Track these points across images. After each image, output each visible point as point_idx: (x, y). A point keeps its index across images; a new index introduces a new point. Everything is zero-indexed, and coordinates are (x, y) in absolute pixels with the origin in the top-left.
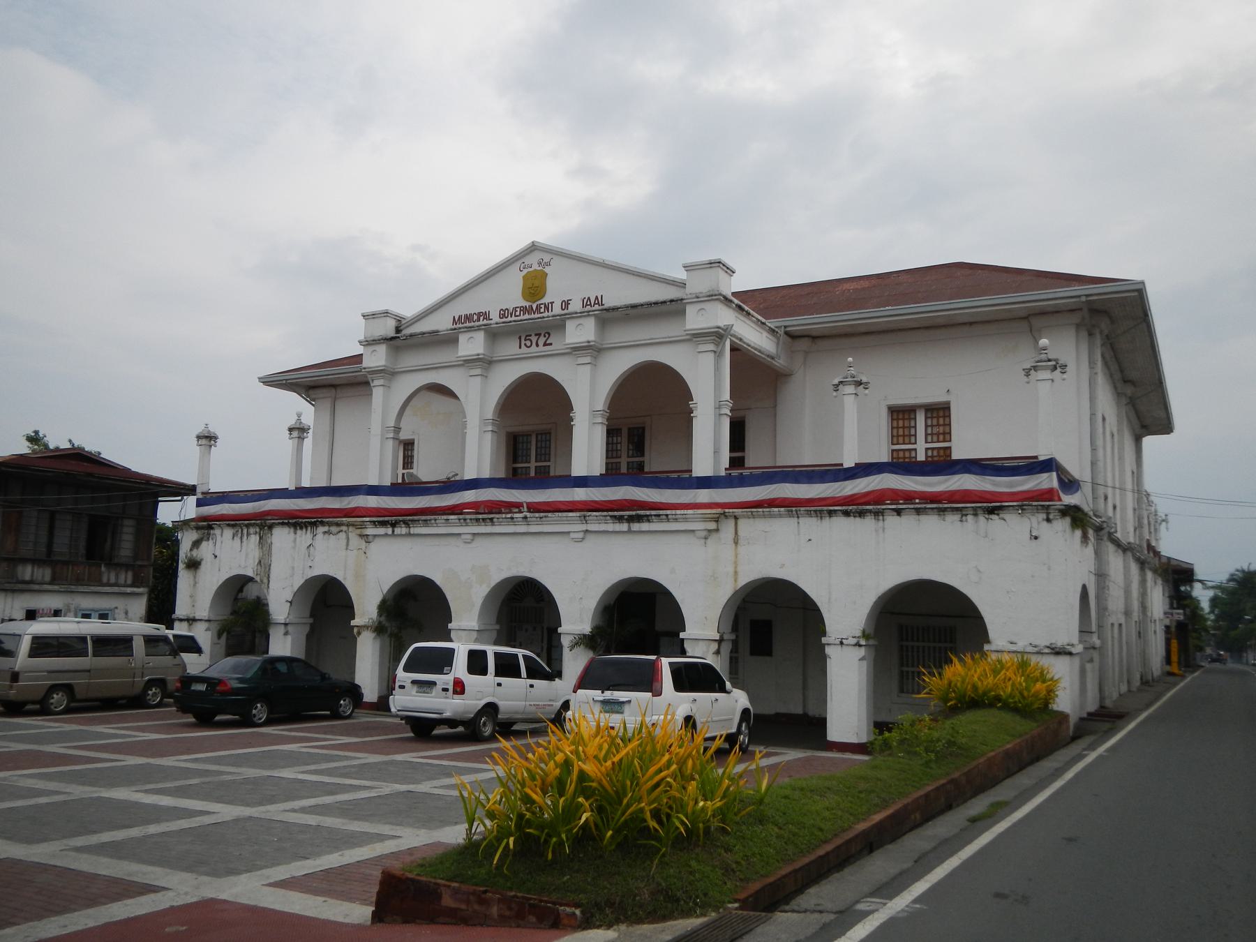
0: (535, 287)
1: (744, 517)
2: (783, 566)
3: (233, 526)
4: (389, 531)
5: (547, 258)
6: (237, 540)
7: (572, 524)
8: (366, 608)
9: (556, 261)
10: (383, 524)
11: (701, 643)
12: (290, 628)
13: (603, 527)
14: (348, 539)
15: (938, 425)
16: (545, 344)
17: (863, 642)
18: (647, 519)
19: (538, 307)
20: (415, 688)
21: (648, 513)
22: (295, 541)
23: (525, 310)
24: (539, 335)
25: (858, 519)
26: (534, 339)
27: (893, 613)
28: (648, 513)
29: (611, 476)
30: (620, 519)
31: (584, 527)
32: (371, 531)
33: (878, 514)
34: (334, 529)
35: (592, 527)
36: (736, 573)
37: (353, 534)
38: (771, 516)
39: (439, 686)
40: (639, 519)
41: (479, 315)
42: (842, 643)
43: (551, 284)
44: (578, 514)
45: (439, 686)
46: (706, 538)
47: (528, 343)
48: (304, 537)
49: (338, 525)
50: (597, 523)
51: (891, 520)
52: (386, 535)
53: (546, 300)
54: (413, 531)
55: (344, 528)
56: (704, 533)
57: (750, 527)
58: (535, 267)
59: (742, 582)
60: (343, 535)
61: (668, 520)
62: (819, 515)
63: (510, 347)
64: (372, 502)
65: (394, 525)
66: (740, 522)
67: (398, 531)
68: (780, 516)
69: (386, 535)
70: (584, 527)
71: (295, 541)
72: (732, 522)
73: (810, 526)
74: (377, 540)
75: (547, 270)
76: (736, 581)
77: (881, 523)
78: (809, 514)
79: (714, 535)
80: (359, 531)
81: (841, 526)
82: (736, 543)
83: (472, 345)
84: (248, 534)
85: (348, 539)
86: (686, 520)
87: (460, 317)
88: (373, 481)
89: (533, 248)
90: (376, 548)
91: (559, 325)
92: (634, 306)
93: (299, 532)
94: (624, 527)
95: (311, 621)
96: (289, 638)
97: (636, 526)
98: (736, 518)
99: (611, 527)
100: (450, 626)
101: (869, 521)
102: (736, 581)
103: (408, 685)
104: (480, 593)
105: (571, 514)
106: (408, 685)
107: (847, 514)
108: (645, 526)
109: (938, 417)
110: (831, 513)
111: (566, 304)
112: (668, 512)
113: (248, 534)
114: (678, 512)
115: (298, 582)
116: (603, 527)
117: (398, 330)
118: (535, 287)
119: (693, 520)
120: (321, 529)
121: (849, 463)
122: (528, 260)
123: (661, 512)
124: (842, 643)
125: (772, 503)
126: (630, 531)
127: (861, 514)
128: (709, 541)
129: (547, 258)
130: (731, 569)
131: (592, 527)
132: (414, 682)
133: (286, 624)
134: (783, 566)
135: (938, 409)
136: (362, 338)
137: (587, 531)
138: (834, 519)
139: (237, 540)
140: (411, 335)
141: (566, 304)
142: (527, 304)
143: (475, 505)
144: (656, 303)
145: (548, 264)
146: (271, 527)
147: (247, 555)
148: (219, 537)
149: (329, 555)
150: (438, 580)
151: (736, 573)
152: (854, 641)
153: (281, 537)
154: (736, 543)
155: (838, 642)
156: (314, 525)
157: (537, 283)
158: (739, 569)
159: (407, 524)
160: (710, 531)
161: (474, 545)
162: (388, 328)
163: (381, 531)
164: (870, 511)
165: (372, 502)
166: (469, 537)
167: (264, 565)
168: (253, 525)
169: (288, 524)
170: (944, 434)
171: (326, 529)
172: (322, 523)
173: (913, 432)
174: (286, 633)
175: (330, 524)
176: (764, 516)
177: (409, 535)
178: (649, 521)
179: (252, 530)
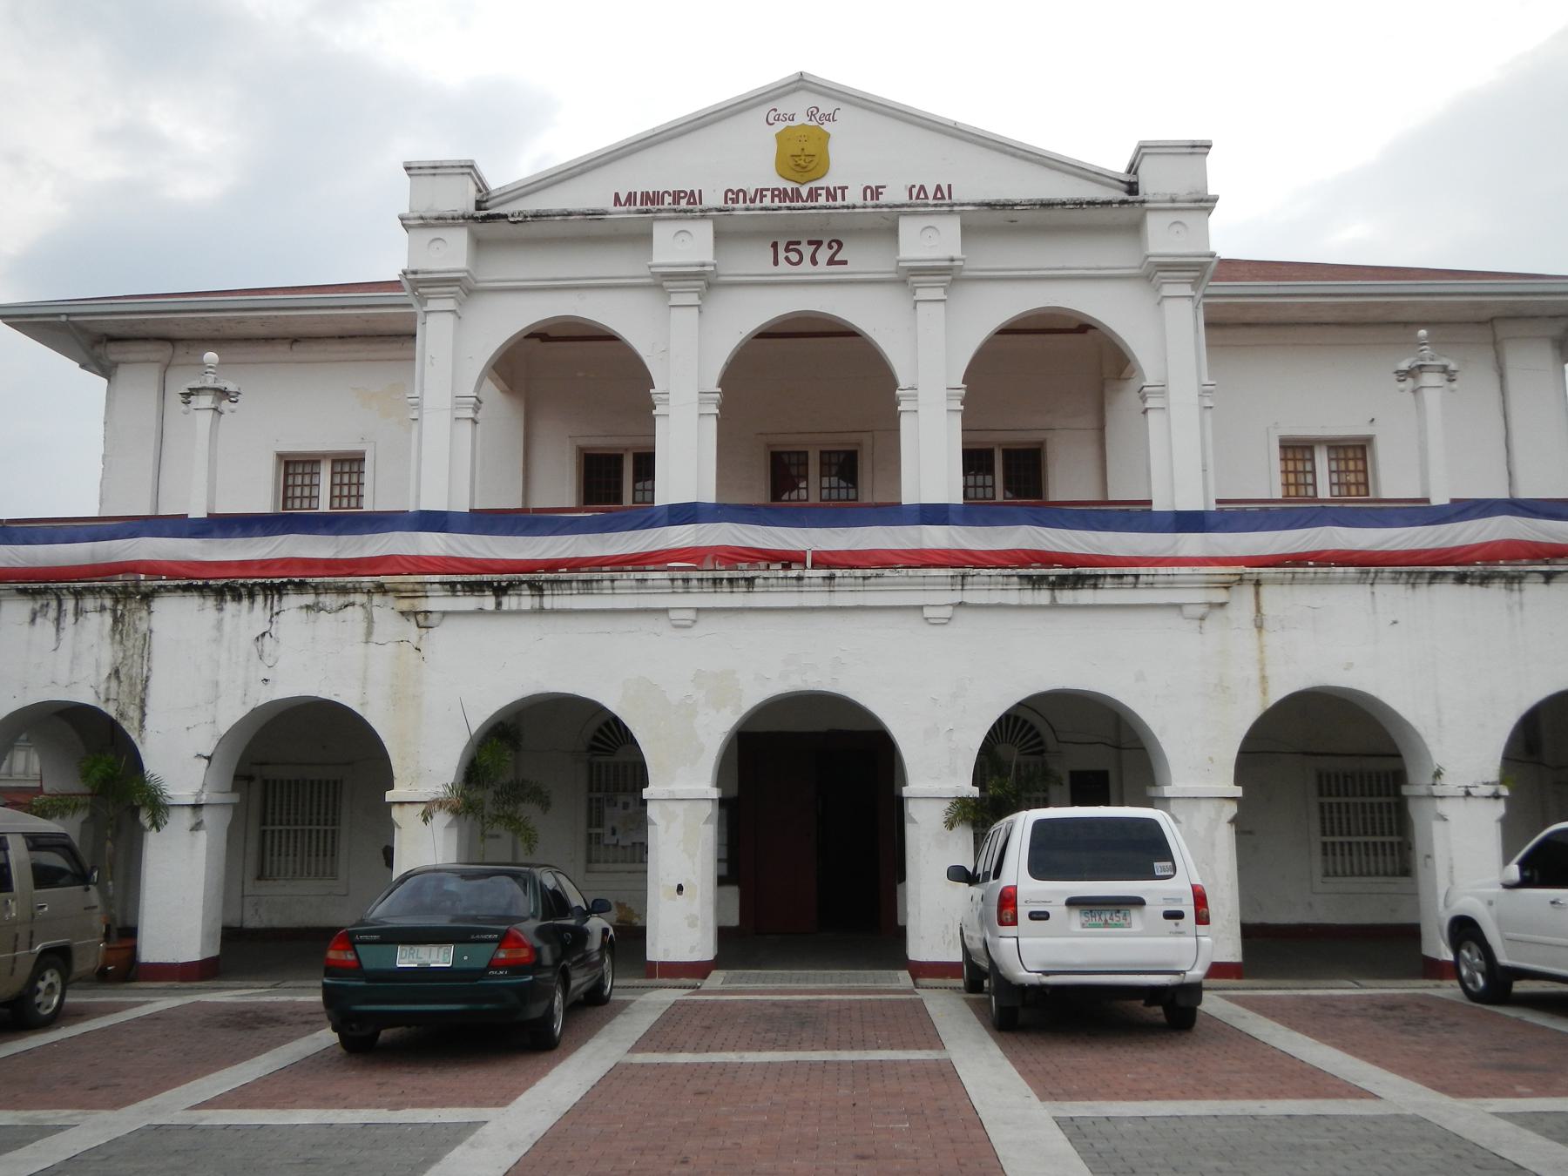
0: (803, 157)
1: (1274, 582)
2: (1349, 666)
3: (35, 594)
4: (489, 602)
5: (826, 107)
7: (936, 590)
8: (426, 760)
9: (847, 114)
10: (474, 588)
11: (1204, 805)
12: (206, 815)
13: (997, 597)
14: (370, 621)
15: (1347, 471)
16: (831, 262)
17: (1504, 791)
18: (1094, 582)
19: (813, 194)
20: (1076, 918)
21: (1100, 571)
23: (782, 194)
24: (819, 244)
25: (1477, 588)
26: (807, 250)
27: (1305, 753)
28: (1100, 571)
29: (972, 512)
30: (1036, 582)
31: (957, 597)
32: (437, 602)
33: (1512, 580)
34: (329, 600)
35: (970, 597)
36: (1264, 678)
37: (385, 611)
38: (1327, 581)
39: (1154, 908)
40: (1077, 582)
41: (677, 196)
42: (1468, 794)
43: (836, 151)
44: (951, 572)
45: (1154, 908)
46: (1202, 619)
47: (794, 257)
48: (246, 618)
49: (343, 590)
50: (984, 589)
51: (1534, 591)
52: (480, 611)
53: (829, 181)
54: (548, 602)
55: (359, 598)
56: (1201, 610)
57: (1281, 599)
58: (801, 119)
59: (1277, 693)
60: (355, 614)
61: (1135, 586)
62: (1413, 580)
63: (756, 261)
64: (433, 544)
65: (500, 591)
66: (1266, 591)
67: (509, 602)
68: (1343, 581)
69: (480, 611)
70: (957, 597)
71: (220, 622)
72: (1248, 591)
73: (1392, 597)
74: (449, 622)
75: (827, 127)
76: (1264, 692)
77: (1516, 595)
78: (1395, 580)
79: (1218, 613)
80: (405, 605)
81: (1447, 598)
82: (1260, 627)
83: (682, 245)
84: (78, 612)
85: (370, 621)
86: (1170, 585)
87: (631, 198)
88: (434, 501)
89: (801, 84)
90: (443, 639)
91: (882, 225)
92: (1047, 205)
93: (230, 606)
94: (1043, 597)
95: (235, 798)
96: (202, 835)
97: (1066, 596)
98: (1258, 583)
99: (1013, 597)
100: (646, 793)
101: (1496, 591)
102: (1264, 692)
103: (1058, 910)
104: (715, 729)
105: (934, 572)
106: (1058, 910)
107: (1461, 579)
108: (1085, 596)
109: (1347, 460)
110: (1435, 578)
112: (1142, 570)
113: (78, 612)
114: (1162, 570)
115: (232, 712)
116: (997, 597)
117: (479, 205)
118: (803, 157)
119: (1188, 585)
120: (292, 601)
121: (1440, 498)
122: (784, 106)
123: (1127, 570)
124: (1468, 794)
125: (1299, 560)
126: (1053, 605)
127: (1485, 580)
128: (1207, 623)
129: (826, 107)
130: (1254, 674)
131: (970, 597)
132: (1072, 903)
133: (196, 807)
134: (1349, 666)
135: (1345, 448)
136: (405, 211)
137: (961, 604)
138: (1436, 587)
140: (537, 216)
142: (789, 186)
143: (694, 555)
144: (1091, 203)
145: (831, 118)
146: (148, 597)
147: (75, 659)
149: (313, 654)
150: (612, 701)
151: (1264, 678)
152: (1489, 790)
153: (177, 621)
154: (1260, 627)
155: (1461, 792)
156: (279, 590)
157: (810, 150)
158: (1269, 672)
159: (537, 589)
160: (1211, 605)
161: (697, 631)
162: (460, 198)
163: (468, 602)
164: (1503, 575)
165: (433, 544)
166: (691, 615)
167: (131, 676)
168: (92, 591)
169: (201, 590)
170: (1357, 484)
171: (309, 599)
172: (301, 587)
173: (1335, 479)
174: (196, 827)
175: (316, 589)
176: (1312, 582)
177: (541, 611)
178: (1095, 587)
179: (89, 603)
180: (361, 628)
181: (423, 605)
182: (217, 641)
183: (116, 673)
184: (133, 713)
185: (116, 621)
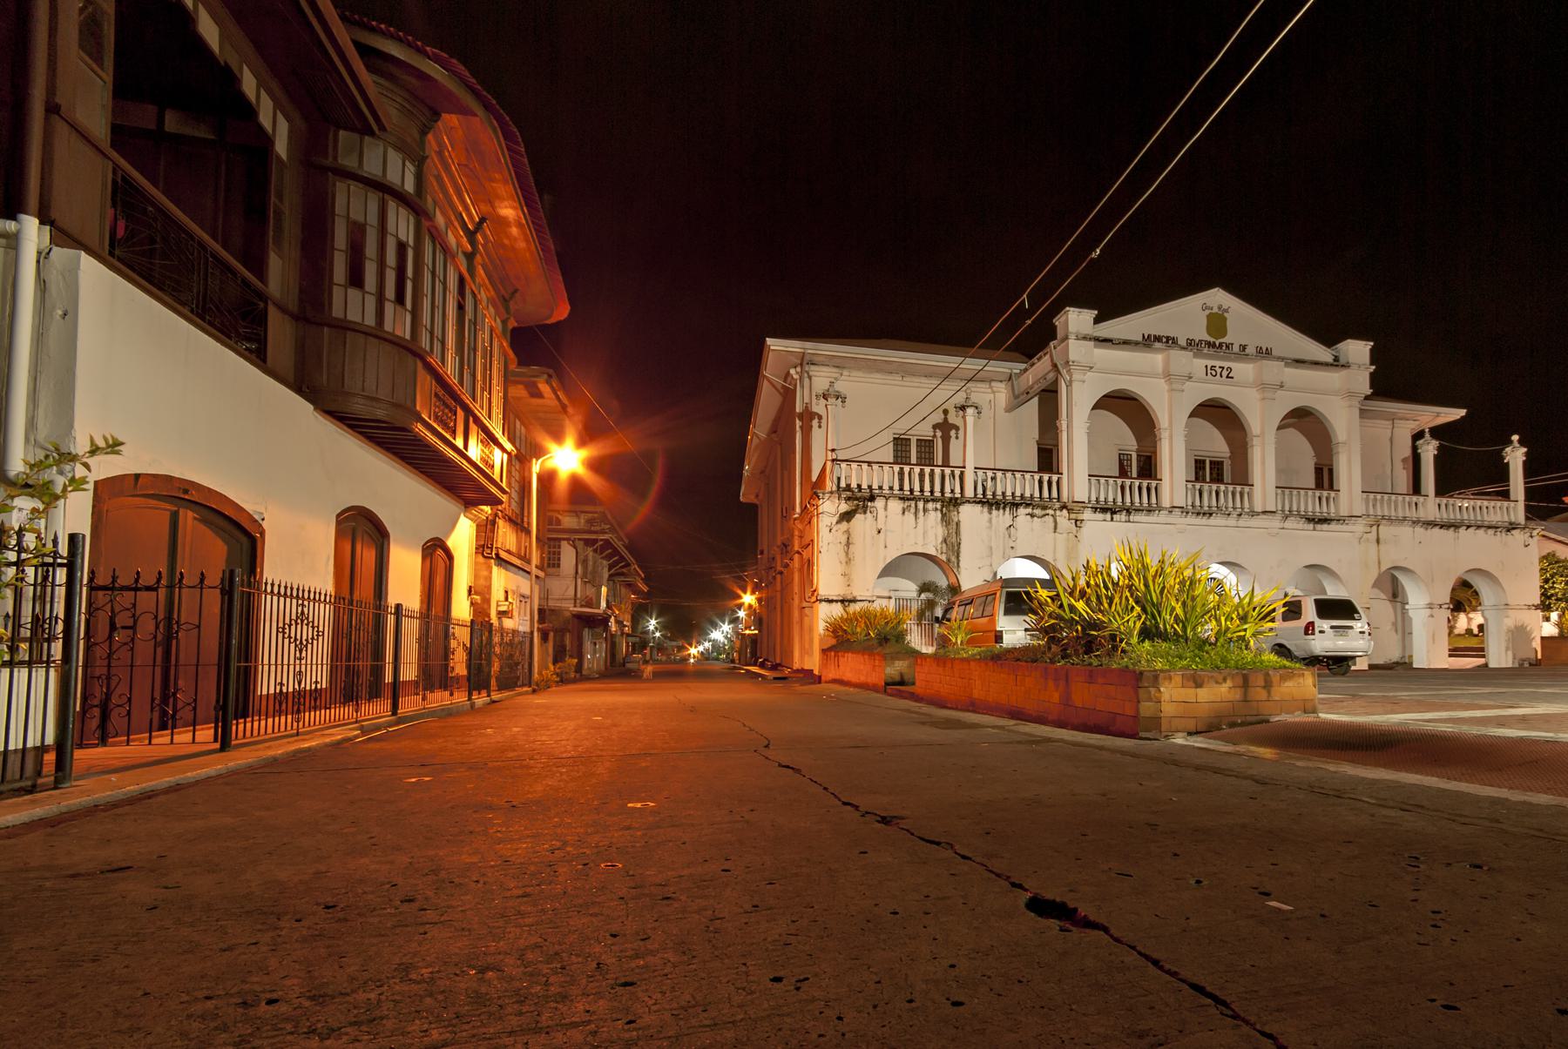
6: (910, 516)
19: (1221, 345)
22: (990, 521)
34: (1038, 512)
41: (1168, 338)
48: (1002, 518)
53: (1225, 340)
58: (1215, 310)
60: (1049, 519)
67: (1116, 517)
71: (990, 521)
93: (994, 512)
111: (1243, 348)
113: (925, 510)
120: (1022, 511)
139: (910, 516)
141: (1243, 348)
147: (925, 533)
148: (881, 512)
167: (953, 544)
171: (1029, 510)
179: (930, 505)
180: (1052, 525)
181: (1080, 517)
182: (990, 528)
183: (945, 541)
184: (953, 559)
185: (944, 516)
